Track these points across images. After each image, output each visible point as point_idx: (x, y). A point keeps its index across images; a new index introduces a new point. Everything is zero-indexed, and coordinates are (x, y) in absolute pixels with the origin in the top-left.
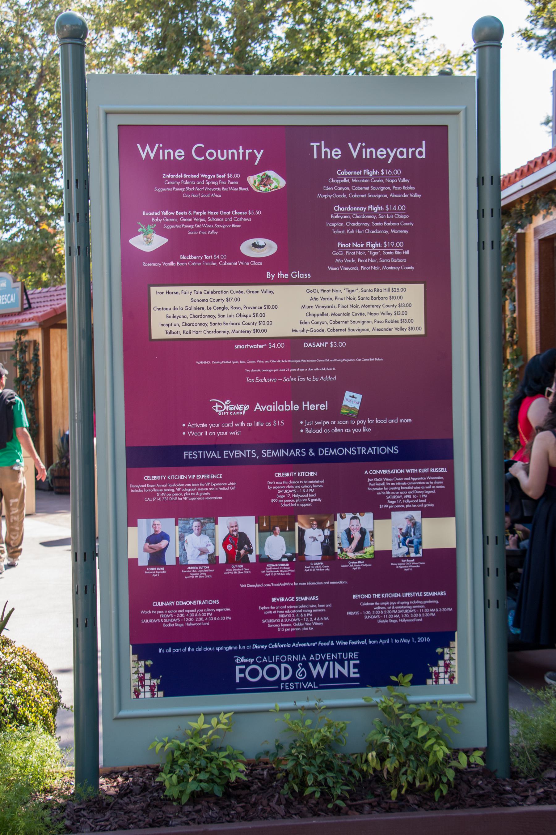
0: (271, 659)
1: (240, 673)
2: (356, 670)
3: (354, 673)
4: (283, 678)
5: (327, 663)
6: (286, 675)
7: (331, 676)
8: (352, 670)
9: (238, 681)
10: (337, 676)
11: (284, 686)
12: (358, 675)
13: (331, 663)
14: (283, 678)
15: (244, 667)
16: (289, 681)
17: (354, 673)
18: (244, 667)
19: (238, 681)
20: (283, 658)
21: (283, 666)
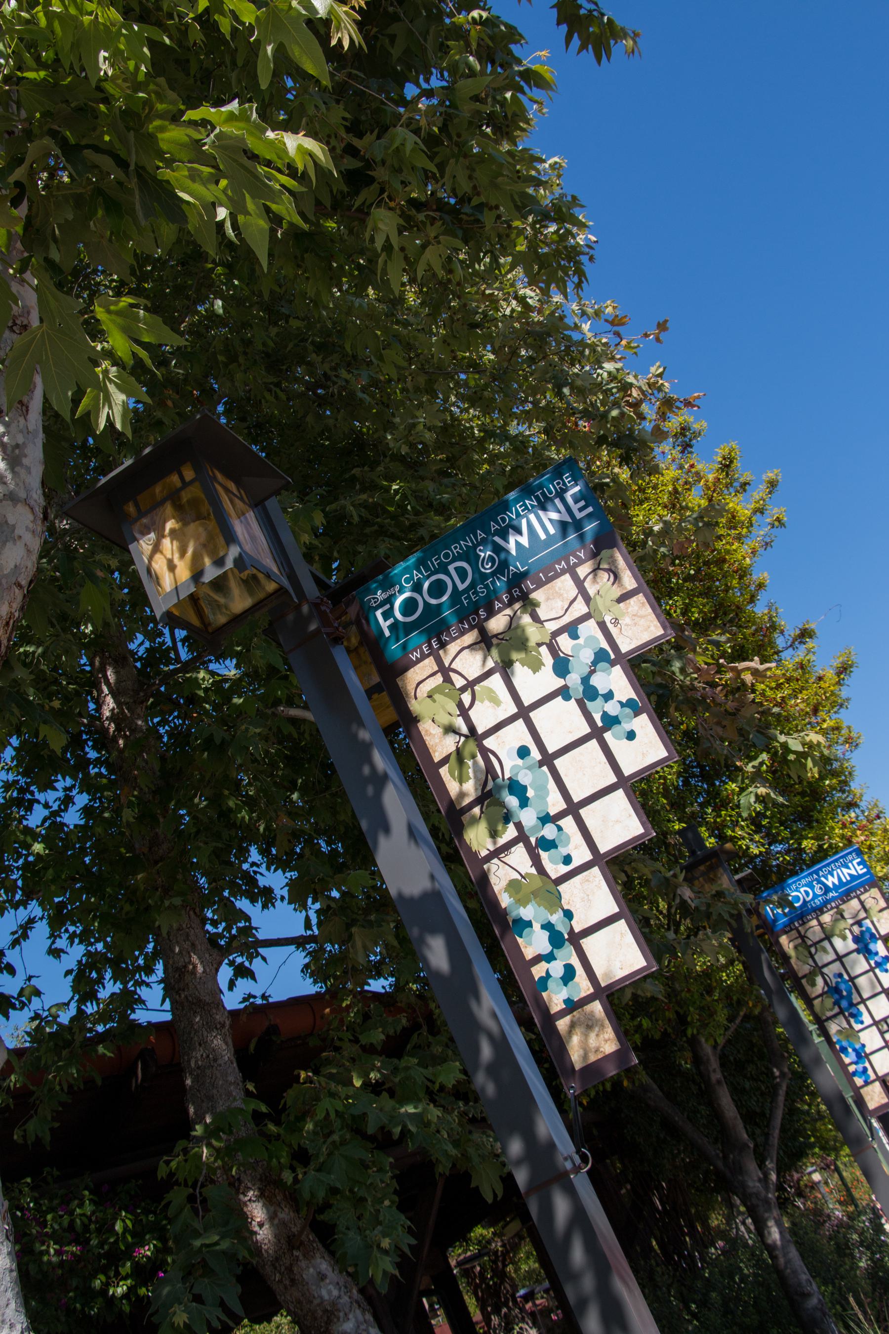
0: (427, 569)
1: (385, 620)
2: (582, 503)
3: (581, 510)
4: (461, 587)
5: (524, 522)
6: (463, 579)
7: (543, 536)
8: (575, 508)
9: (387, 633)
10: (552, 531)
11: (469, 597)
12: (590, 509)
13: (532, 517)
14: (461, 587)
15: (388, 606)
16: (473, 586)
17: (581, 510)
18: (388, 606)
19: (387, 633)
20: (447, 556)
21: (451, 568)
